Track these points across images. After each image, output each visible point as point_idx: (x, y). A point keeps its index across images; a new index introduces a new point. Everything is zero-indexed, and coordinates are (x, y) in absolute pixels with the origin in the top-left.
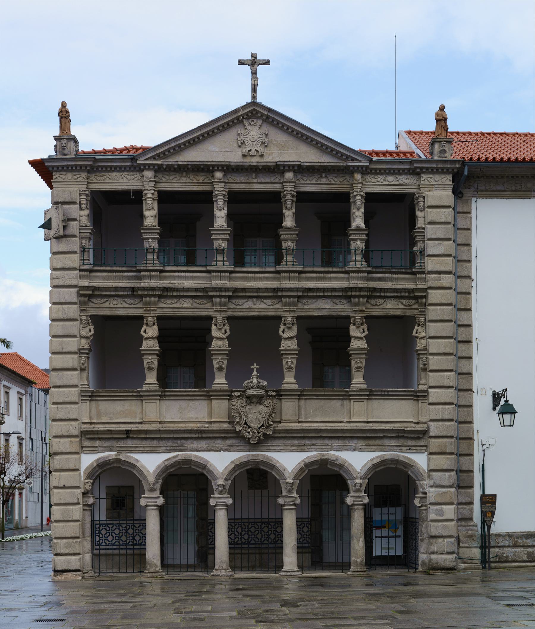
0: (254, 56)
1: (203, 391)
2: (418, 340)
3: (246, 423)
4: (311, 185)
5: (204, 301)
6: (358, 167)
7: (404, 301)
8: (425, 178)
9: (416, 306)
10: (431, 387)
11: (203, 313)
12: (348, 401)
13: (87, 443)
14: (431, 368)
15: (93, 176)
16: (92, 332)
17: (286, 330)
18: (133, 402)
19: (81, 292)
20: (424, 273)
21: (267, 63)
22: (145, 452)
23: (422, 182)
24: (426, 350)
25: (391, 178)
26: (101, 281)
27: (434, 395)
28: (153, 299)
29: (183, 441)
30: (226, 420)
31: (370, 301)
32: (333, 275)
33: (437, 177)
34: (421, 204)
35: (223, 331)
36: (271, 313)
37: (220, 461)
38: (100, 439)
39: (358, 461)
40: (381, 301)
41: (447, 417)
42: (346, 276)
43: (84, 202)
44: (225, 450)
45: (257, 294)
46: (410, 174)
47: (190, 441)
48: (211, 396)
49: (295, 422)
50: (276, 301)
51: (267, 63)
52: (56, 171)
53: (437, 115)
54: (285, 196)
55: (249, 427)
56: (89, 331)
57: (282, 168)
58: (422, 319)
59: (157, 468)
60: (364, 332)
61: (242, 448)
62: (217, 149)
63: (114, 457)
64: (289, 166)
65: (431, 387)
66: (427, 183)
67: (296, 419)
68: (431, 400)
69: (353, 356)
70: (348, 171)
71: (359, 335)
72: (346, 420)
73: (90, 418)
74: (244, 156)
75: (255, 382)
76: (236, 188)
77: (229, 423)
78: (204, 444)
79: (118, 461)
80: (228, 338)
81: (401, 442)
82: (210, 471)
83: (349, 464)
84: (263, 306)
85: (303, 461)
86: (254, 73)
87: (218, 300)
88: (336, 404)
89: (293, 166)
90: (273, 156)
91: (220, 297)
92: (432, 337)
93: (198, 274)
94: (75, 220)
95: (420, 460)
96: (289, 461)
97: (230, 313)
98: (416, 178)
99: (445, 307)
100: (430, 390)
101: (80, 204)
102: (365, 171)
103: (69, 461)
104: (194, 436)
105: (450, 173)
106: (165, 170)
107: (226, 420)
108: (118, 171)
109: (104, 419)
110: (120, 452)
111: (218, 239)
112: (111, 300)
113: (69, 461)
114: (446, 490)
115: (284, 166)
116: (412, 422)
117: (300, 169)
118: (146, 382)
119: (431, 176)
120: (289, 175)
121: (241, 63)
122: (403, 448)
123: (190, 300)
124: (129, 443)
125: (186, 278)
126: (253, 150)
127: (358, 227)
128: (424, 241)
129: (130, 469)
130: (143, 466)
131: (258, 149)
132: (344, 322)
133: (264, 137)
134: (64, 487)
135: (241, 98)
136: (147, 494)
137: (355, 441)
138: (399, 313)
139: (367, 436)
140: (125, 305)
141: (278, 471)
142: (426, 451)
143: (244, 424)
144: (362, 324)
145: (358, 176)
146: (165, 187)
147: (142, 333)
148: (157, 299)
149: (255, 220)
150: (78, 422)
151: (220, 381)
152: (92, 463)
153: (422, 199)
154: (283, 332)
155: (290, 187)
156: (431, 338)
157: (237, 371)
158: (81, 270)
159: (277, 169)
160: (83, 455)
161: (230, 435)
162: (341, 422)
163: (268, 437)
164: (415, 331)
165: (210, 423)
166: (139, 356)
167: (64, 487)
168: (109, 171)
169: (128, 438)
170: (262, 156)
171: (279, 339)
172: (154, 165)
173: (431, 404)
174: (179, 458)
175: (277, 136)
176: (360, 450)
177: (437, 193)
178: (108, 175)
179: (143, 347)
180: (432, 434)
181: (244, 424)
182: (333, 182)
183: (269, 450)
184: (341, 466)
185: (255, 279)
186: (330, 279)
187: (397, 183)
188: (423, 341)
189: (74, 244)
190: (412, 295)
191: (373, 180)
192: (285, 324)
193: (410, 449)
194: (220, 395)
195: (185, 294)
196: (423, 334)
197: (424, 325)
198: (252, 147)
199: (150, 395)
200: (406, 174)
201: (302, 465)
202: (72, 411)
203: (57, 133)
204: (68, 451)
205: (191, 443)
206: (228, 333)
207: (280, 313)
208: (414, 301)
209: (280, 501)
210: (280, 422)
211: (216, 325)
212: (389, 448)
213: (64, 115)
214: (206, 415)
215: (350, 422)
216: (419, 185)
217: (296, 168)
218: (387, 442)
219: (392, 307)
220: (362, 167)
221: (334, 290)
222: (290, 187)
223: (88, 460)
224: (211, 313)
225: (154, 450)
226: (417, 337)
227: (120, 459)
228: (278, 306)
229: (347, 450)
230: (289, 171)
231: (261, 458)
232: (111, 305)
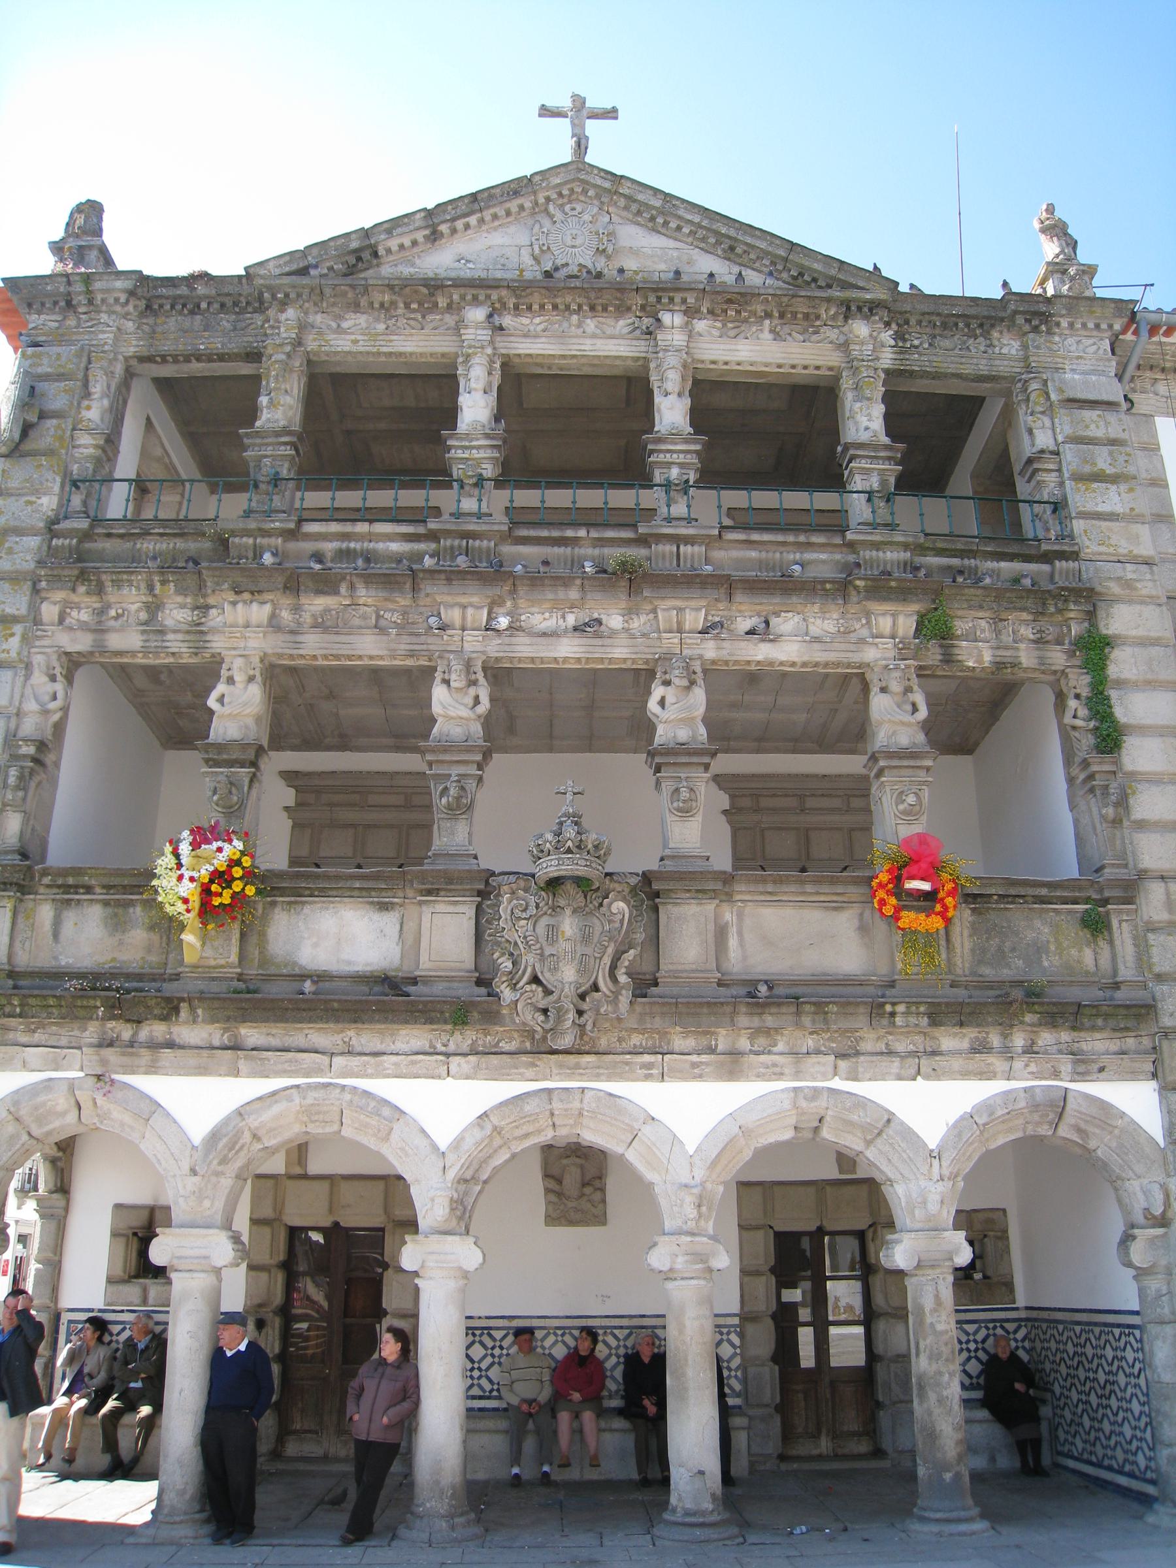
3: (535, 980)
21: (611, 114)
35: (469, 701)
51: (611, 114)
55: (548, 992)
60: (915, 709)
121: (546, 112)
143: (529, 983)
147: (212, 703)
149: (577, 434)
154: (662, 703)
181: (529, 983)
206: (485, 705)
211: (447, 682)
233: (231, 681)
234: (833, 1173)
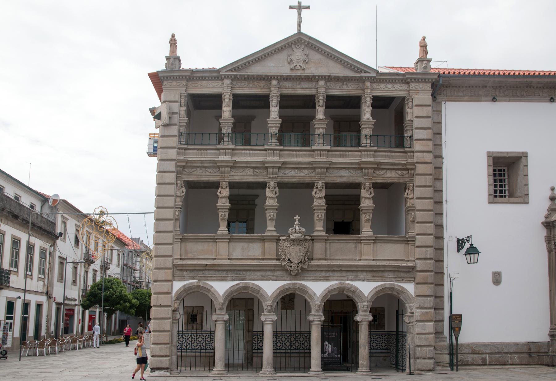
0: (299, 3)
1: (259, 236)
2: (408, 200)
4: (337, 90)
5: (262, 171)
6: (368, 77)
7: (399, 172)
9: (407, 176)
10: (418, 235)
11: (261, 179)
12: (359, 244)
13: (178, 273)
14: (417, 220)
15: (190, 83)
16: (184, 193)
17: (318, 192)
18: (211, 244)
19: (178, 164)
21: (308, 7)
22: (217, 280)
23: (411, 89)
24: (414, 207)
25: (390, 86)
26: (193, 156)
27: (420, 240)
28: (227, 169)
29: (244, 273)
30: (275, 257)
31: (375, 172)
32: (350, 153)
33: (421, 85)
34: (410, 104)
35: (274, 192)
36: (307, 180)
37: (270, 288)
38: (186, 270)
39: (366, 288)
40: (384, 172)
41: (428, 256)
42: (359, 153)
43: (183, 101)
44: (273, 280)
45: (298, 167)
46: (403, 83)
47: (249, 273)
48: (265, 239)
49: (322, 259)
50: (311, 171)
51: (308, 7)
52: (166, 80)
53: (421, 43)
54: (318, 98)
56: (182, 191)
57: (317, 77)
58: (411, 185)
60: (371, 194)
62: (274, 65)
64: (322, 76)
65: (418, 235)
66: (414, 89)
67: (323, 257)
68: (418, 243)
70: (362, 80)
71: (368, 196)
72: (358, 258)
73: (180, 255)
74: (292, 69)
75: (296, 230)
76: (286, 92)
77: (277, 260)
78: (258, 274)
79: (198, 286)
80: (277, 197)
81: (396, 274)
82: (262, 295)
83: (360, 291)
84: (302, 174)
85: (327, 288)
86: (299, 14)
87: (271, 170)
88: (352, 246)
89: (325, 76)
90: (311, 71)
91: (273, 167)
92: (417, 198)
93: (258, 152)
94: (176, 113)
95: (410, 288)
96: (318, 289)
97: (279, 180)
98: (407, 86)
99: (427, 177)
100: (417, 237)
101: (180, 102)
102: (374, 80)
103: (164, 287)
105: (430, 82)
107: (275, 257)
108: (207, 80)
110: (200, 280)
111: (273, 127)
112: (198, 169)
114: (428, 311)
115: (319, 76)
116: (403, 260)
117: (329, 79)
118: (220, 229)
119: (417, 84)
120: (322, 83)
122: (398, 279)
124: (206, 273)
125: (250, 155)
126: (298, 66)
127: (368, 119)
128: (412, 130)
129: (206, 293)
131: (301, 65)
132: (358, 186)
133: (305, 57)
134: (161, 306)
135: (288, 30)
136: (218, 312)
137: (364, 274)
138: (396, 180)
139: (373, 271)
140: (207, 173)
141: (310, 296)
142: (414, 281)
144: (370, 188)
145: (368, 84)
146: (238, 91)
147: (218, 193)
148: (229, 169)
151: (271, 229)
152: (180, 288)
153: (411, 100)
154: (316, 193)
156: (417, 198)
157: (284, 222)
158: (178, 149)
160: (174, 282)
161: (277, 269)
163: (304, 270)
164: (406, 193)
165: (263, 259)
166: (215, 211)
167: (161, 306)
168: (201, 80)
170: (304, 69)
171: (312, 198)
173: (417, 247)
174: (241, 285)
176: (368, 280)
177: (422, 96)
178: (200, 83)
179: (218, 204)
180: (418, 269)
182: (351, 88)
183: (304, 280)
184: (354, 292)
185: (297, 156)
186: (348, 156)
187: (394, 89)
188: (412, 201)
189: (174, 130)
190: (405, 167)
191: (378, 87)
192: (317, 188)
193: (403, 280)
194: (271, 239)
195: (249, 165)
196: (412, 196)
197: (413, 190)
199: (222, 239)
200: (400, 83)
201: (327, 291)
203: (168, 54)
204: (163, 279)
205: (250, 275)
206: (278, 194)
207: (313, 180)
208: (406, 172)
209: (311, 318)
210: (312, 259)
211: (269, 188)
212: (388, 279)
213: (173, 42)
214: (260, 254)
215: (360, 260)
216: (409, 91)
217: (327, 78)
218: (387, 274)
219: (391, 176)
220: (371, 77)
221: (352, 163)
222: (322, 91)
223: (178, 286)
224: (266, 179)
226: (408, 198)
227: (200, 286)
228: (312, 175)
229: (359, 280)
230: (322, 79)
231: (298, 286)
232: (198, 173)
233: (222, 187)
234: (346, 298)
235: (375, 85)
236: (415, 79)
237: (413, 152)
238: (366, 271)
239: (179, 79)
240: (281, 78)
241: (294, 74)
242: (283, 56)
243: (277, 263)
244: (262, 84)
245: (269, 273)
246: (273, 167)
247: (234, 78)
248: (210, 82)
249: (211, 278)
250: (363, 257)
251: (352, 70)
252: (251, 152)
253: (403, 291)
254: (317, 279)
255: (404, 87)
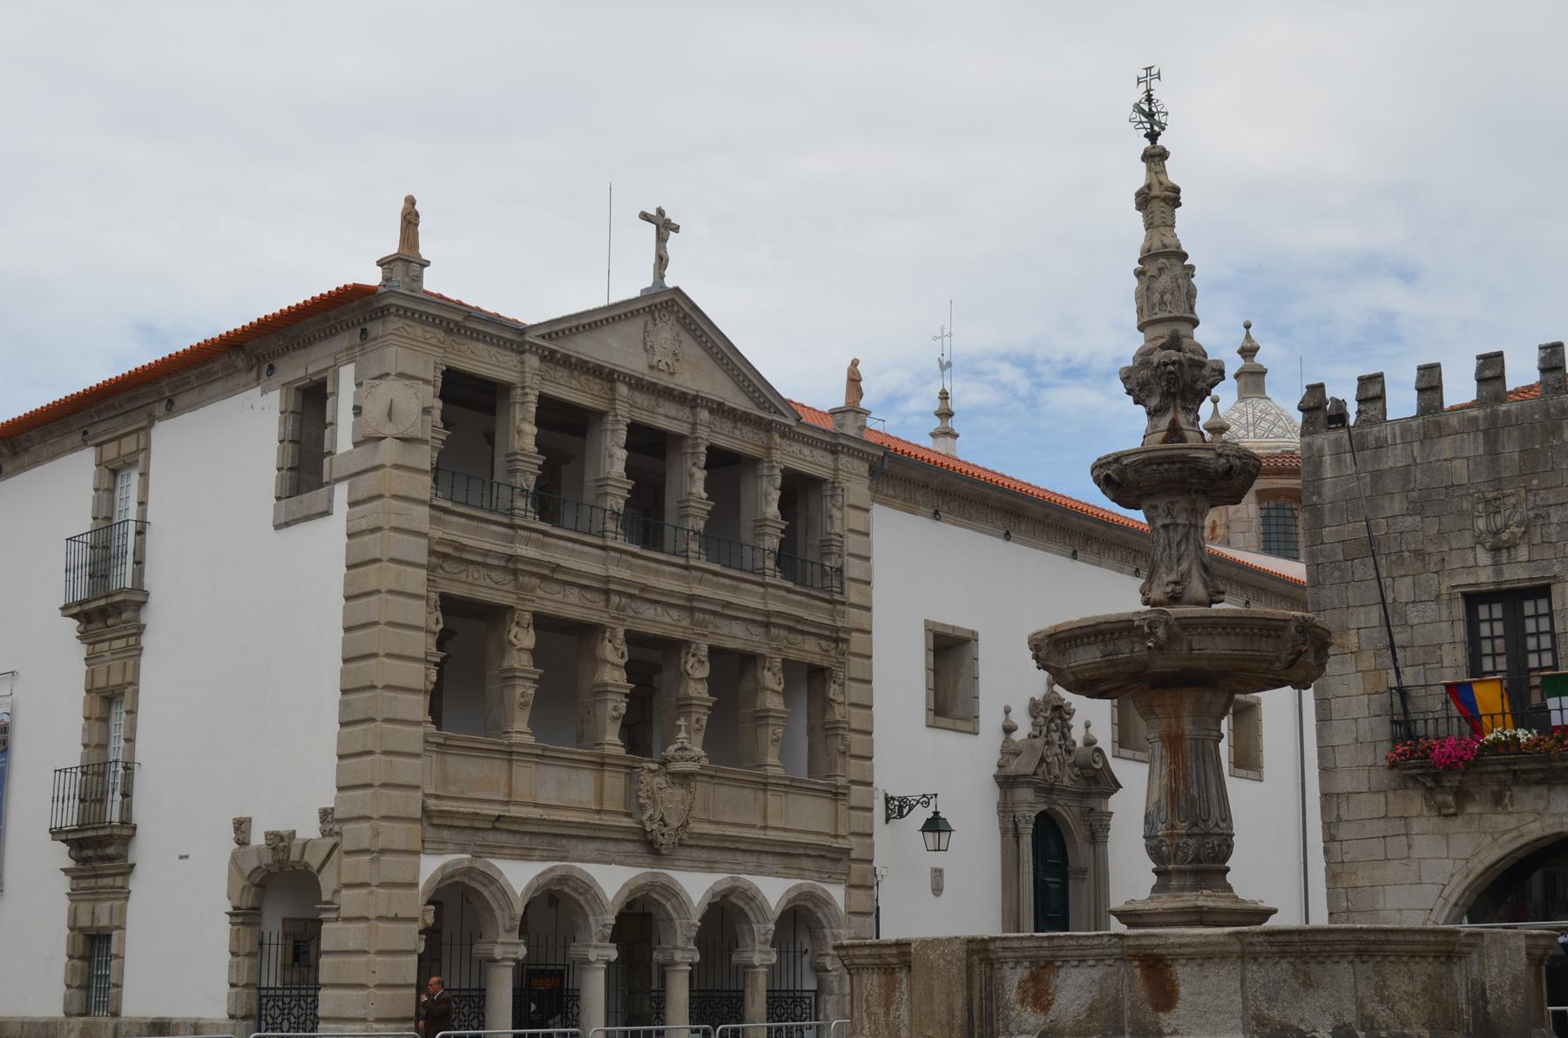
7: (824, 644)
8: (844, 460)
10: (853, 782)
11: (594, 617)
13: (431, 833)
20: (843, 603)
29: (564, 842)
32: (747, 586)
36: (677, 634)
37: (612, 880)
40: (800, 638)
42: (762, 590)
45: (664, 602)
47: (573, 843)
59: (528, 888)
61: (640, 860)
63: (466, 864)
65: (853, 782)
69: (771, 721)
77: (627, 815)
78: (592, 847)
84: (667, 619)
91: (620, 594)
96: (696, 886)
102: (788, 433)
104: (583, 833)
106: (557, 363)
109: (453, 790)
110: (476, 856)
113: (392, 867)
123: (576, 591)
124: (492, 838)
130: (509, 885)
134: (396, 919)
139: (786, 855)
140: (489, 582)
150: (420, 794)
155: (702, 432)
159: (688, 401)
162: (753, 826)
167: (396, 919)
169: (494, 829)
170: (672, 374)
172: (544, 348)
173: (851, 808)
174: (558, 872)
175: (691, 349)
180: (853, 855)
188: (841, 708)
198: (662, 357)
202: (407, 770)
204: (403, 847)
207: (689, 636)
215: (765, 828)
218: (806, 863)
223: (430, 867)
225: (525, 855)
229: (762, 874)
232: (470, 579)
235: (785, 442)
236: (849, 448)
237: (843, 603)
238: (774, 853)
239: (433, 325)
240: (638, 384)
241: (651, 377)
242: (634, 328)
243: (627, 822)
244: (596, 385)
245: (612, 847)
246: (620, 594)
247: (549, 358)
248: (494, 350)
249: (499, 851)
250: (771, 823)
251: (752, 399)
252: (577, 547)
253: (827, 902)
254: (694, 869)
255: (828, 459)
